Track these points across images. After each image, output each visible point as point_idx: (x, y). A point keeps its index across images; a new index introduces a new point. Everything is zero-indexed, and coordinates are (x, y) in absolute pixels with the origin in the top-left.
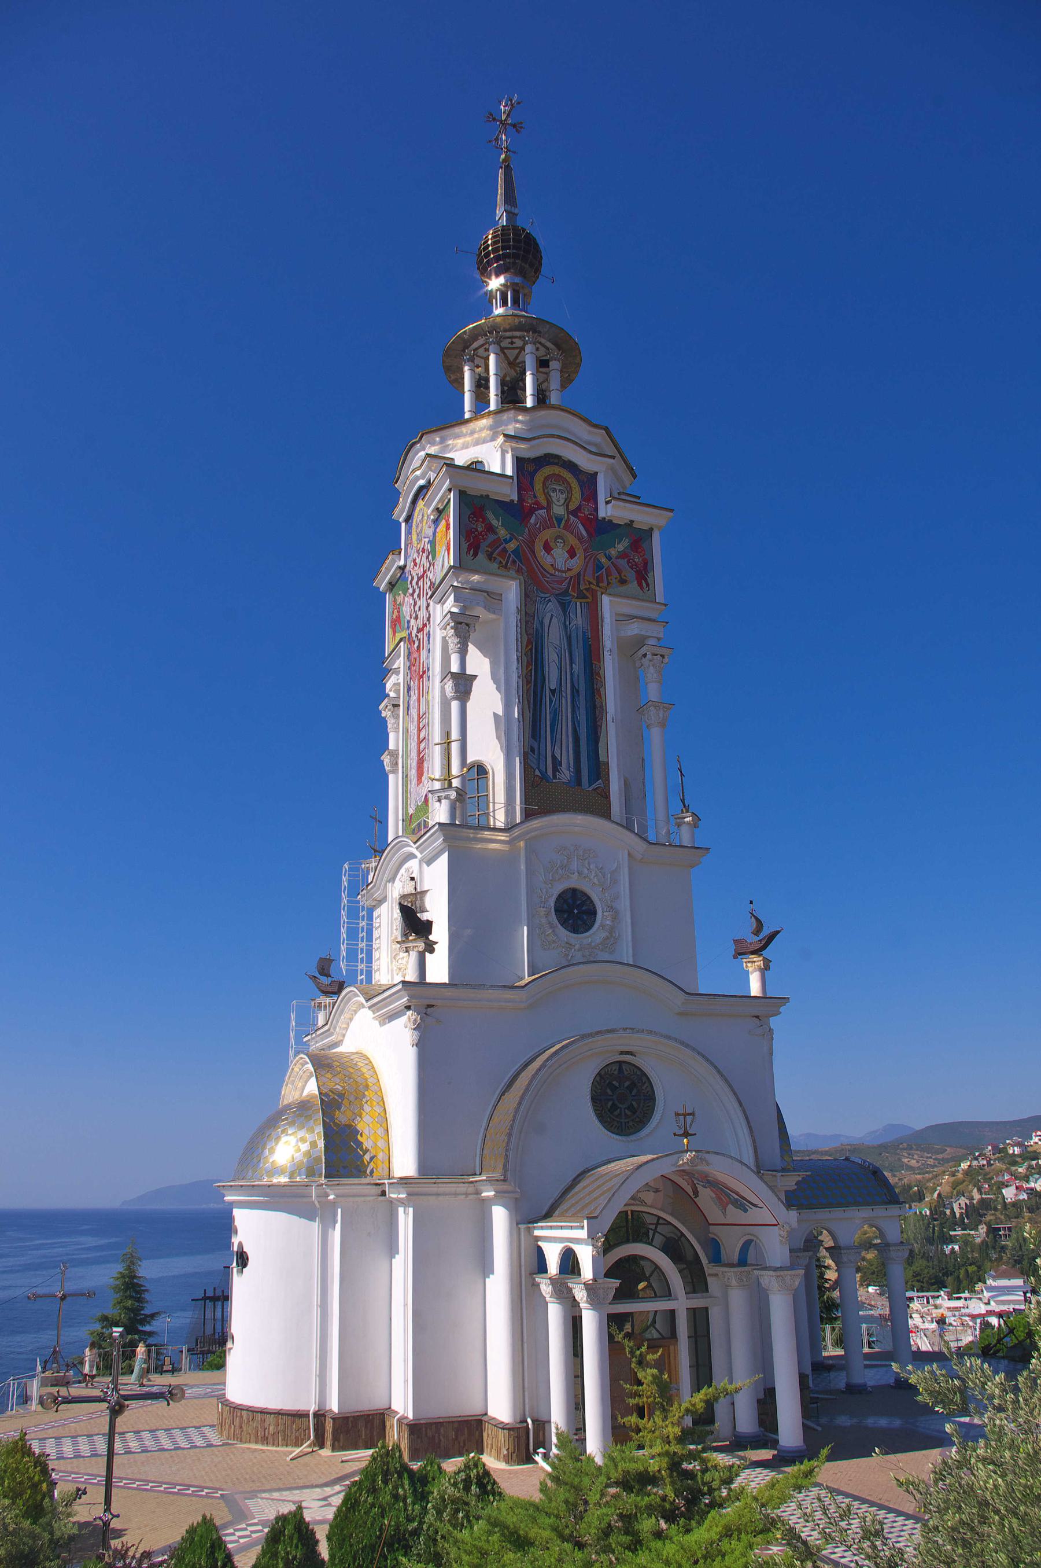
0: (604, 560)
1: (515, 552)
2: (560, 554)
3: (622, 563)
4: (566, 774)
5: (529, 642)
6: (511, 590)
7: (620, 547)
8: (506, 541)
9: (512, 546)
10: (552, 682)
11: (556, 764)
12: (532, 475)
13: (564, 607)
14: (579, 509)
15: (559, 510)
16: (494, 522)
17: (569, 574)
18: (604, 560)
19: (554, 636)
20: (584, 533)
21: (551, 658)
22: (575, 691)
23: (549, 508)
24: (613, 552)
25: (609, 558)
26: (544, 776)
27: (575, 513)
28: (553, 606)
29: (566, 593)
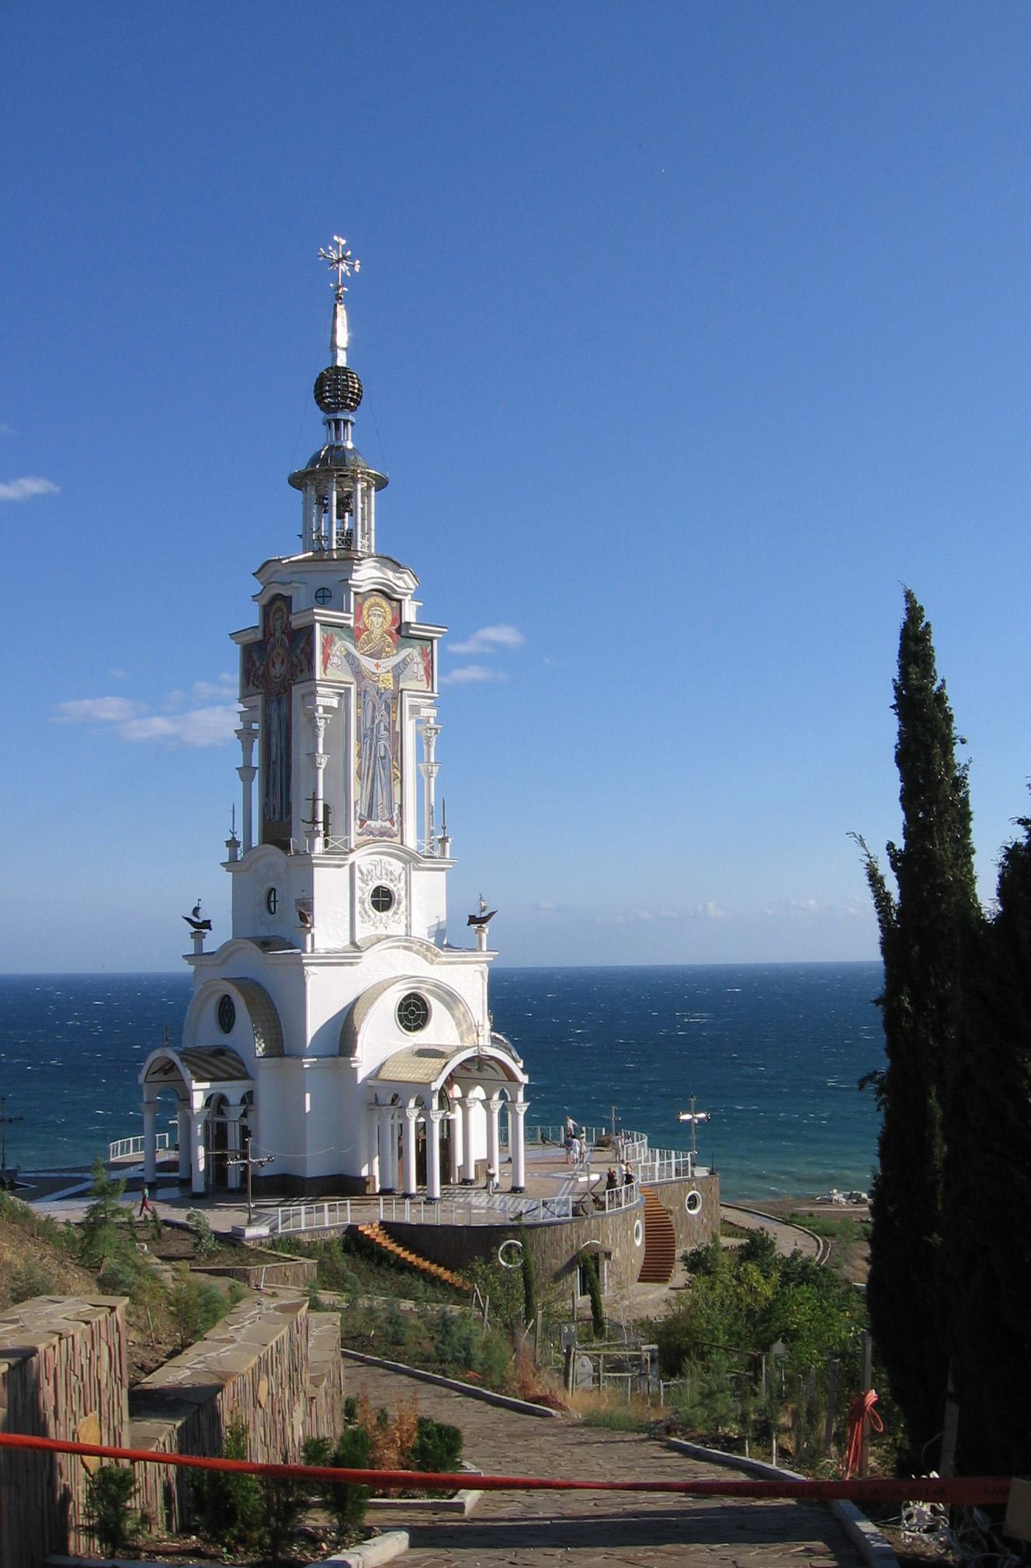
0: (295, 659)
1: (262, 675)
2: (278, 666)
3: (302, 657)
4: (277, 816)
5: (266, 735)
6: (258, 700)
7: (301, 646)
8: (259, 669)
9: (260, 672)
10: (273, 758)
11: (274, 809)
12: (270, 612)
13: (279, 702)
14: (285, 629)
15: (278, 634)
16: (255, 658)
17: (282, 677)
18: (295, 659)
19: (275, 725)
20: (288, 645)
21: (274, 740)
22: (282, 758)
23: (274, 636)
24: (298, 651)
25: (297, 657)
26: (270, 820)
27: (283, 633)
28: (274, 705)
29: (280, 693)
